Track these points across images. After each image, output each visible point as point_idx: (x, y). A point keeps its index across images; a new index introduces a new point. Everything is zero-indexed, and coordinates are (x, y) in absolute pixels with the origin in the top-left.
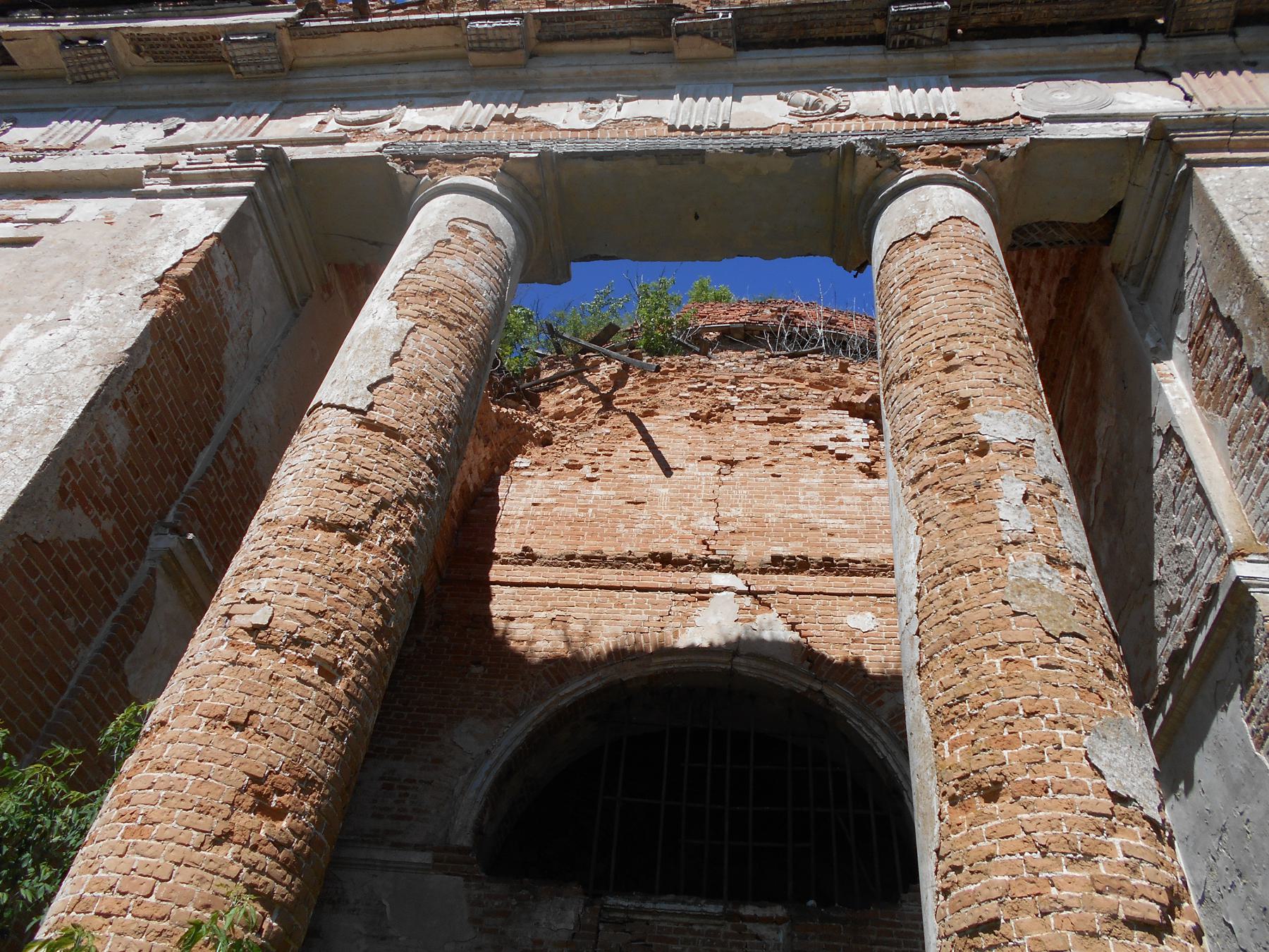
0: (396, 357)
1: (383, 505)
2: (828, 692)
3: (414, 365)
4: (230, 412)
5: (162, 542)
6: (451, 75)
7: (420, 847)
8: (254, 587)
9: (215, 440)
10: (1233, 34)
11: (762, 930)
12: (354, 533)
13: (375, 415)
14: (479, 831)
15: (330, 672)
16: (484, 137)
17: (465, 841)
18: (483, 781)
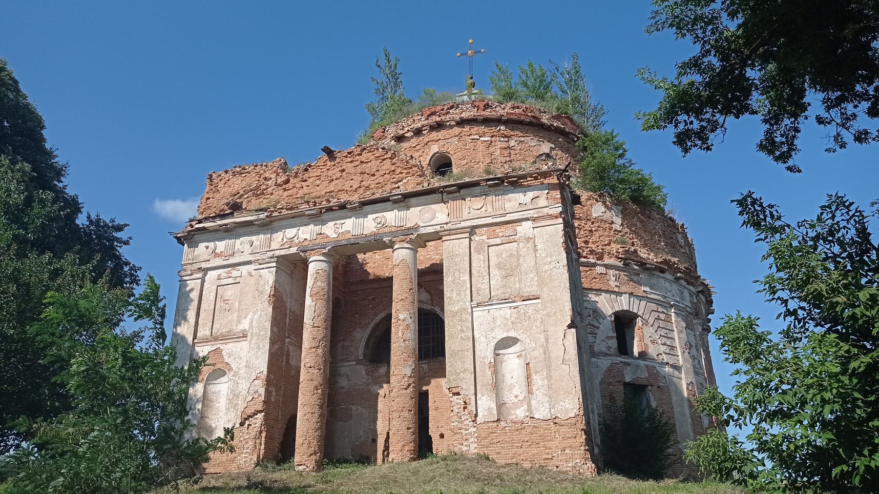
0: (315, 311)
1: (320, 341)
2: (436, 309)
3: (318, 312)
4: (288, 308)
5: (287, 340)
6: (305, 220)
7: (353, 361)
8: (307, 360)
9: (288, 315)
10: (459, 192)
11: (423, 366)
12: (317, 347)
13: (315, 325)
14: (364, 355)
15: (320, 369)
16: (317, 241)
17: (362, 358)
18: (363, 343)
